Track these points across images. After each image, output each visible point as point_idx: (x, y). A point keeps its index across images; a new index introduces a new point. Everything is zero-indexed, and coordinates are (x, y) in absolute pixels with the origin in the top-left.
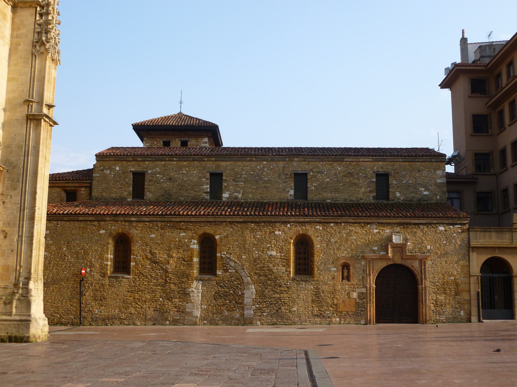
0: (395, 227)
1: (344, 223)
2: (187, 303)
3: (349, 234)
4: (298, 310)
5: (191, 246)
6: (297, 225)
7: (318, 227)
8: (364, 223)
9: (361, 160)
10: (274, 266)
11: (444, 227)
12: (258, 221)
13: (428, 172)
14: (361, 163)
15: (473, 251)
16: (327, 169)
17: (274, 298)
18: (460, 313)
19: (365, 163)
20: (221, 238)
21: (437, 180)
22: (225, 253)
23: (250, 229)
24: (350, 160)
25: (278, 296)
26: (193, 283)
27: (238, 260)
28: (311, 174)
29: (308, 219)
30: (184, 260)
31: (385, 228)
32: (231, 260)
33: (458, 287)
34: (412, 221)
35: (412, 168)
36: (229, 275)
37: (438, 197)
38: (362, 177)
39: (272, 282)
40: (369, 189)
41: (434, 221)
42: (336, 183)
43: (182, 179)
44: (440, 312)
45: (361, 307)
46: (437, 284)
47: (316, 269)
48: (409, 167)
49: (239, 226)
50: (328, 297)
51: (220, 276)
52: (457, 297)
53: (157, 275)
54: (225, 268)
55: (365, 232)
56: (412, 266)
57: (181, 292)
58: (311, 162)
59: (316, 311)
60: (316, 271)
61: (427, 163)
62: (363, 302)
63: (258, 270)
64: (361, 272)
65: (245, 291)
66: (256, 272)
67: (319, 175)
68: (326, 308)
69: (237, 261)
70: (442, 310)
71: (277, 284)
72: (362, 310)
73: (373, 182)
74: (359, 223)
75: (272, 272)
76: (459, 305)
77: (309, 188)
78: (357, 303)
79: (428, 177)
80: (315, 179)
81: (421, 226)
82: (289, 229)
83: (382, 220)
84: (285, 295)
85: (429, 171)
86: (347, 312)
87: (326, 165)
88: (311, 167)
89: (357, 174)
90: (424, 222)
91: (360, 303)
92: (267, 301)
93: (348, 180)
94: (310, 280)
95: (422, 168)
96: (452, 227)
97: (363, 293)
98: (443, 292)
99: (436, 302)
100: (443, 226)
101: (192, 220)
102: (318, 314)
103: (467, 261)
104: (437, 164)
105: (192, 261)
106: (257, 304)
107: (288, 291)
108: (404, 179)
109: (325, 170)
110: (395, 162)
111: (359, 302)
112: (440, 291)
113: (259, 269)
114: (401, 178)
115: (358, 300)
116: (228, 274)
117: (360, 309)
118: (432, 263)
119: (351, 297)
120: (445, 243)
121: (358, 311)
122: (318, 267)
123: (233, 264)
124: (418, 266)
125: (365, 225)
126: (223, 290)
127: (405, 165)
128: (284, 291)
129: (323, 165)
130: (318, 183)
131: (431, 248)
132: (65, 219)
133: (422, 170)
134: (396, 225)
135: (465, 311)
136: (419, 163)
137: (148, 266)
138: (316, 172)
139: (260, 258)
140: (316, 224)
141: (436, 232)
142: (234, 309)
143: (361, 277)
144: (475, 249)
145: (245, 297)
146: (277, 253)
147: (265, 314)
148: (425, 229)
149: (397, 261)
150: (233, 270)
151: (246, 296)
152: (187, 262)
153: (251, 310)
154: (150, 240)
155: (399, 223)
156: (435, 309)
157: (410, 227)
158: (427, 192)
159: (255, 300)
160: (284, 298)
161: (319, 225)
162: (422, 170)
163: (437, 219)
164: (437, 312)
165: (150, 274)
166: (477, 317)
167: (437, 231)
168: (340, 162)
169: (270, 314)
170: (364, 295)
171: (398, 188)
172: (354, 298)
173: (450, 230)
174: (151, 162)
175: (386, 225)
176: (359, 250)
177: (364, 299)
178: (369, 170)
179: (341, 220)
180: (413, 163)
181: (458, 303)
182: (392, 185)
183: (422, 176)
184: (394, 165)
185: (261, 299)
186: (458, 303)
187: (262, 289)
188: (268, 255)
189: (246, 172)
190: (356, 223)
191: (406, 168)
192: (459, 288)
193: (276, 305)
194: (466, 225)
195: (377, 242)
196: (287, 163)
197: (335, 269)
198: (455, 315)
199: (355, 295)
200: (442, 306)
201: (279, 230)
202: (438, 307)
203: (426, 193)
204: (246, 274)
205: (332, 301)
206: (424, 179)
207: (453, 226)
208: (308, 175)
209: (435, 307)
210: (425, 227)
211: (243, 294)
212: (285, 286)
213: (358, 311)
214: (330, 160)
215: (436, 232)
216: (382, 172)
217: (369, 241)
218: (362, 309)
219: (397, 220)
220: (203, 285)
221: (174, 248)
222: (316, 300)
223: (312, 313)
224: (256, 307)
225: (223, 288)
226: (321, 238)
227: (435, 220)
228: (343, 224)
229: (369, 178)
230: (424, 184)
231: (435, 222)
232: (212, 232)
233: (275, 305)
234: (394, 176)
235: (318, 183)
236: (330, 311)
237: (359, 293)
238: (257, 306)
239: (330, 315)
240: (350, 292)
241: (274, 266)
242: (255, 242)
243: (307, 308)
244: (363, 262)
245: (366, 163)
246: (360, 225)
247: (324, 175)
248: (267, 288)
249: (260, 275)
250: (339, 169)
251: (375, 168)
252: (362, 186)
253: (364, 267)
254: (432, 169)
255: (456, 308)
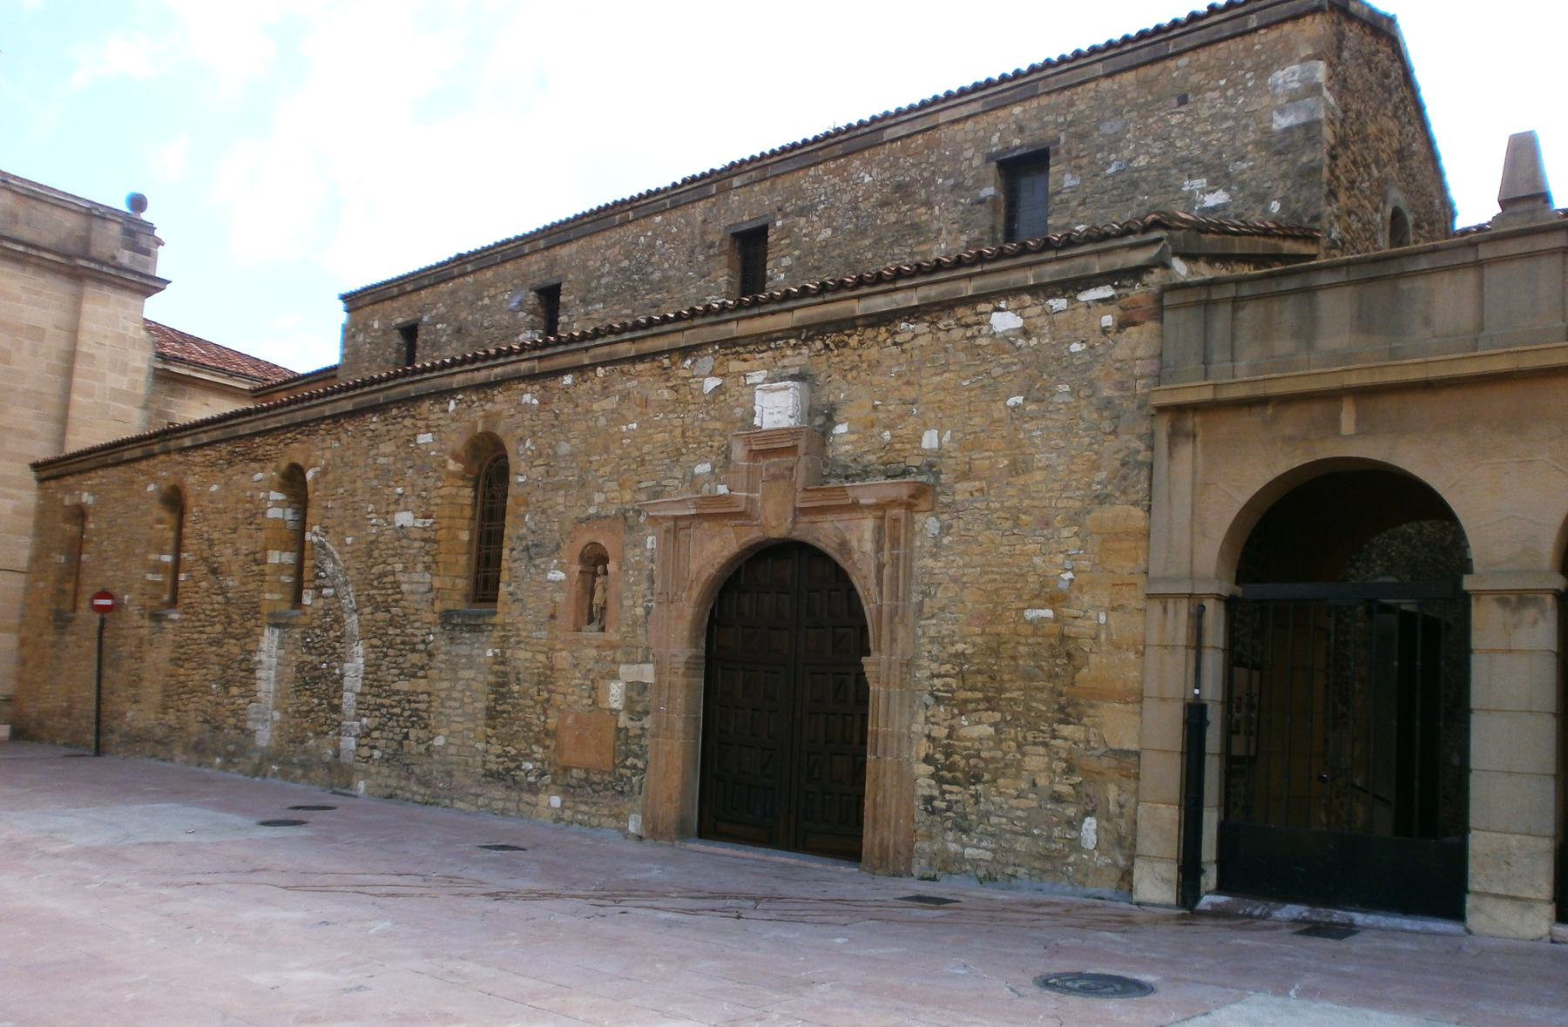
0: (789, 352)
1: (603, 364)
2: (251, 702)
3: (617, 417)
4: (448, 744)
5: (273, 513)
6: (474, 398)
7: (527, 398)
8: (670, 352)
9: (943, 117)
10: (405, 570)
11: (1019, 311)
12: (381, 401)
13: (1230, 93)
14: (941, 134)
15: (1174, 436)
16: (826, 194)
17: (397, 693)
18: (1079, 831)
19: (956, 127)
20: (315, 479)
21: (1271, 120)
22: (316, 528)
23: (369, 434)
24: (903, 133)
25: (403, 685)
26: (262, 634)
27: (340, 553)
28: (779, 223)
29: (498, 370)
30: (255, 560)
31: (746, 366)
32: (330, 555)
33: (1078, 669)
34: (859, 308)
35: (1151, 94)
36: (323, 608)
37: (1275, 207)
38: (943, 191)
39: (398, 631)
40: (964, 238)
41: (962, 284)
42: (852, 240)
43: (482, 324)
44: (964, 816)
45: (636, 756)
46: (960, 647)
47: (504, 576)
48: (1135, 95)
49: (350, 428)
50: (532, 699)
51: (309, 611)
52: (1066, 730)
53: (213, 610)
54: (317, 582)
55: (674, 396)
56: (844, 546)
57: (243, 666)
58: (779, 182)
59: (492, 758)
60: (503, 588)
61: (1222, 45)
62: (642, 729)
63: (374, 588)
64: (644, 586)
65: (347, 665)
66: (368, 595)
67: (803, 221)
68: (522, 745)
69: (337, 556)
70: (977, 802)
71: (407, 639)
72: (634, 767)
73: (982, 202)
74: (654, 355)
75: (401, 592)
76: (1077, 779)
77: (771, 279)
78: (622, 735)
79: (1226, 117)
80: (787, 241)
81: (903, 325)
82: (453, 420)
83: (733, 325)
84: (422, 684)
85: (1235, 85)
86: (587, 771)
87: (826, 178)
88: (779, 198)
89: (928, 183)
90: (913, 299)
91: (631, 733)
92: (383, 706)
93: (892, 218)
94: (485, 624)
95: (1197, 78)
96: (1060, 303)
97: (644, 687)
98: (987, 699)
99: (948, 755)
100: (1013, 305)
101: (269, 424)
102: (500, 769)
103: (1135, 504)
104: (1273, 34)
105: (265, 563)
106: (364, 716)
107: (430, 668)
108: (1113, 156)
109: (820, 196)
110: (1073, 90)
111: (626, 728)
112: (972, 689)
113: (375, 583)
114: (1099, 156)
115: (623, 720)
116: (321, 602)
117: (628, 763)
118: (941, 528)
119: (600, 705)
120: (1017, 406)
121: (623, 771)
122: (510, 569)
123: (329, 567)
124: (868, 546)
125: (674, 364)
126: (309, 658)
127: (1121, 86)
128: (422, 668)
129: (817, 180)
130: (797, 253)
131: (940, 439)
132: (110, 461)
133: (1198, 90)
134: (792, 341)
135: (1109, 820)
136: (1183, 61)
137: (204, 584)
138: (792, 212)
139: (381, 539)
140: (523, 386)
141: (972, 348)
142: (325, 728)
143: (640, 611)
144: (1191, 422)
145: (345, 688)
146: (415, 518)
147: (377, 754)
148: (922, 341)
149: (774, 523)
150: (330, 587)
151: (347, 682)
152: (258, 564)
153: (350, 736)
154: (211, 502)
155: (809, 327)
156: (943, 793)
157: (854, 341)
158: (1221, 191)
159: (361, 699)
160: (418, 694)
161: (529, 388)
162: (1198, 90)
163: (978, 269)
164: (949, 809)
165: (204, 606)
166: (1171, 871)
167: (979, 341)
168: (872, 151)
169: (386, 756)
170: (648, 696)
171: (1083, 203)
172: (611, 710)
173: (1052, 323)
174: (430, 289)
175: (751, 347)
176: (643, 485)
177: (647, 713)
178: (968, 154)
179: (592, 352)
180: (1158, 67)
181: (1070, 770)
182: (1057, 199)
183: (1198, 121)
184: (1071, 104)
185: (374, 696)
186: (1070, 770)
187: (377, 659)
188: (395, 529)
189: (612, 266)
190: (640, 358)
191: (1122, 102)
192: (1079, 676)
193: (401, 723)
194: (1146, 278)
195: (710, 436)
196: (714, 204)
197: (560, 575)
198: (1049, 839)
199: (615, 694)
200: (978, 779)
201: (428, 429)
202: (954, 782)
203: (1211, 200)
204: (351, 602)
205: (543, 718)
206: (1206, 133)
207: (1072, 300)
208: (770, 231)
209: (941, 781)
210: (922, 327)
211: (342, 676)
212: (422, 647)
213: (623, 771)
214: (838, 150)
215: (972, 348)
216: (1021, 147)
217: (683, 433)
218: (636, 761)
219: (798, 314)
220: (281, 645)
221: (243, 523)
222: (498, 708)
223: (484, 763)
224: (361, 726)
225: (310, 654)
226: (534, 443)
227: (970, 277)
228: (600, 371)
229: (967, 189)
230: (1206, 158)
231: (968, 288)
232: (300, 460)
233: (398, 721)
234: (1069, 152)
235: (797, 253)
236: (536, 760)
237: (631, 686)
238: (365, 720)
239: (532, 779)
240: (601, 683)
241: (405, 570)
242: (374, 483)
243: (471, 742)
244: (650, 539)
245: (961, 126)
246: (656, 364)
247: (815, 219)
248: (386, 655)
249: (377, 609)
250: (868, 179)
251: (995, 139)
252: (939, 231)
253: (652, 561)
254: (1249, 71)
255: (1058, 798)
